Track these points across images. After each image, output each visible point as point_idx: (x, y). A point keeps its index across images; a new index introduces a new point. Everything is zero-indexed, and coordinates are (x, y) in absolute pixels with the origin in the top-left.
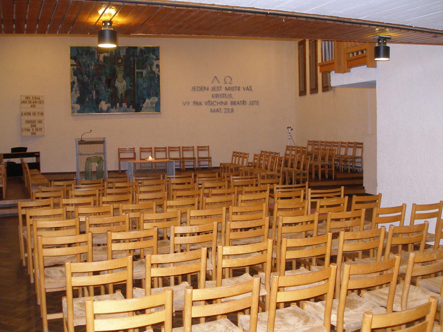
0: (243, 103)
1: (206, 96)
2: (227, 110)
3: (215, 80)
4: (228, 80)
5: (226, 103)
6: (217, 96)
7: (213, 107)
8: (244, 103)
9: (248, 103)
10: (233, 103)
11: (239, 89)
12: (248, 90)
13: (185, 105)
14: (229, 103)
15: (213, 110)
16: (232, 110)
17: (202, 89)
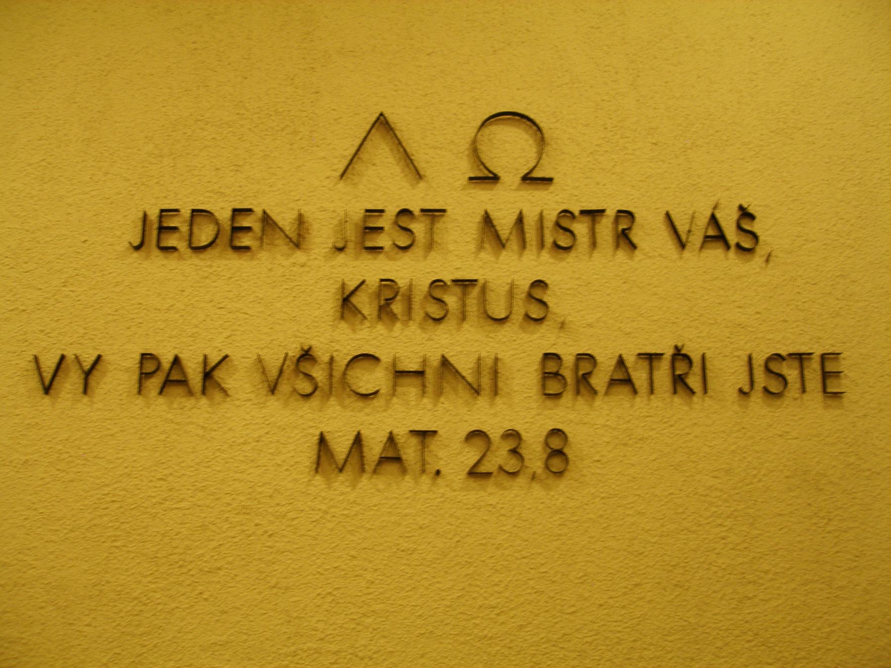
0: (679, 382)
1: (274, 305)
2: (500, 456)
3: (381, 152)
4: (511, 150)
5: (488, 381)
6: (389, 300)
7: (339, 421)
8: (683, 372)
9: (728, 374)
10: (566, 377)
11: (624, 239)
12: (716, 252)
13: (47, 390)
14: (523, 376)
15: (341, 446)
16: (557, 449)
17: (239, 232)
